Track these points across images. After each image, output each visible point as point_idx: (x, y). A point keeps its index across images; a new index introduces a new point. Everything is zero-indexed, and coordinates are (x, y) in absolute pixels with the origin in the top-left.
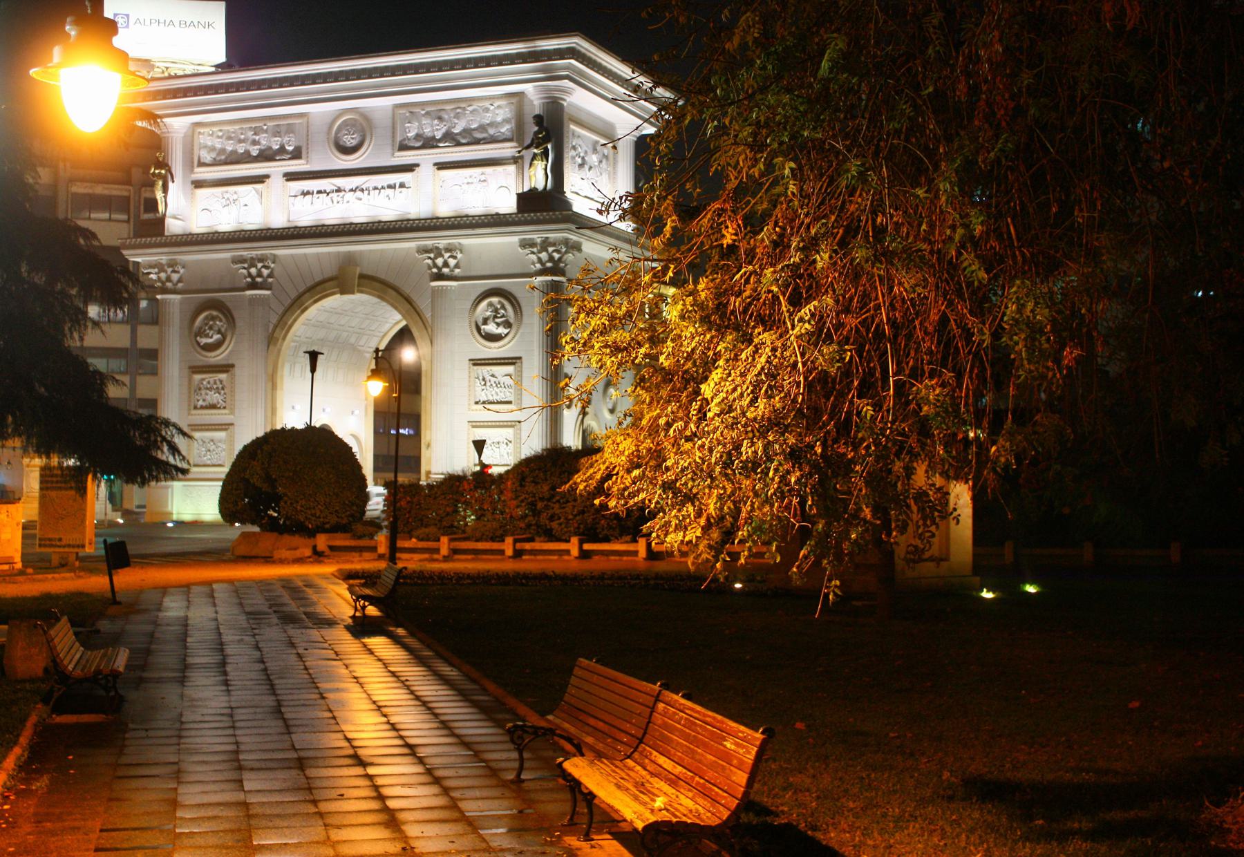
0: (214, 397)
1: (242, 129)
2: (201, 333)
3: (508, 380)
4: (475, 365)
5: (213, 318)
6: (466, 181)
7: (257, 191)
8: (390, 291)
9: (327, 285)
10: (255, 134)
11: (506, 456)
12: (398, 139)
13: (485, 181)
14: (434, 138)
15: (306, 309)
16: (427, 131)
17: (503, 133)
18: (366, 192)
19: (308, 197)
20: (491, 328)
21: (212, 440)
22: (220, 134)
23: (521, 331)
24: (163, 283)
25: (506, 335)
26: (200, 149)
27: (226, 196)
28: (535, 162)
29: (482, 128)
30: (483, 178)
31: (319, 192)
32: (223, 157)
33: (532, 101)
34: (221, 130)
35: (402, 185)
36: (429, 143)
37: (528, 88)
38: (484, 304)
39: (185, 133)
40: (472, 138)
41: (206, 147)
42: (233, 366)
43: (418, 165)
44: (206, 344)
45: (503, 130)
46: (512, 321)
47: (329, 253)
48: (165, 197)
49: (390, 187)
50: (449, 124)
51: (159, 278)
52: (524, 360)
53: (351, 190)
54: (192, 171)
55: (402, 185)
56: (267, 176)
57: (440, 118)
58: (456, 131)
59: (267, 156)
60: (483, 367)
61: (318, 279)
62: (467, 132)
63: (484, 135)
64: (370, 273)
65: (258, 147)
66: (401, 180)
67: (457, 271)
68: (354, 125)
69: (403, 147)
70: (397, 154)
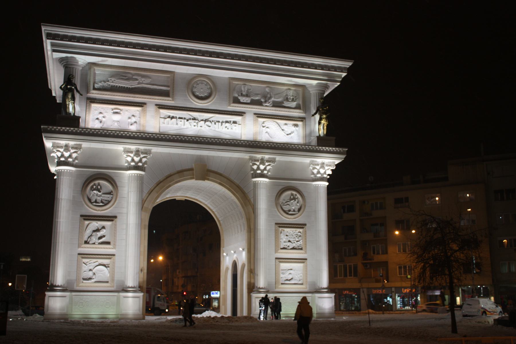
9: (185, 173)
15: (170, 186)
18: (213, 123)
24: (67, 158)
31: (180, 118)
33: (309, 91)
35: (235, 122)
37: (315, 82)
39: (83, 68)
42: (115, 217)
43: (244, 113)
49: (227, 122)
53: (202, 120)
54: (88, 92)
55: (235, 122)
56: (145, 104)
61: (179, 169)
64: (216, 170)
69: (236, 101)
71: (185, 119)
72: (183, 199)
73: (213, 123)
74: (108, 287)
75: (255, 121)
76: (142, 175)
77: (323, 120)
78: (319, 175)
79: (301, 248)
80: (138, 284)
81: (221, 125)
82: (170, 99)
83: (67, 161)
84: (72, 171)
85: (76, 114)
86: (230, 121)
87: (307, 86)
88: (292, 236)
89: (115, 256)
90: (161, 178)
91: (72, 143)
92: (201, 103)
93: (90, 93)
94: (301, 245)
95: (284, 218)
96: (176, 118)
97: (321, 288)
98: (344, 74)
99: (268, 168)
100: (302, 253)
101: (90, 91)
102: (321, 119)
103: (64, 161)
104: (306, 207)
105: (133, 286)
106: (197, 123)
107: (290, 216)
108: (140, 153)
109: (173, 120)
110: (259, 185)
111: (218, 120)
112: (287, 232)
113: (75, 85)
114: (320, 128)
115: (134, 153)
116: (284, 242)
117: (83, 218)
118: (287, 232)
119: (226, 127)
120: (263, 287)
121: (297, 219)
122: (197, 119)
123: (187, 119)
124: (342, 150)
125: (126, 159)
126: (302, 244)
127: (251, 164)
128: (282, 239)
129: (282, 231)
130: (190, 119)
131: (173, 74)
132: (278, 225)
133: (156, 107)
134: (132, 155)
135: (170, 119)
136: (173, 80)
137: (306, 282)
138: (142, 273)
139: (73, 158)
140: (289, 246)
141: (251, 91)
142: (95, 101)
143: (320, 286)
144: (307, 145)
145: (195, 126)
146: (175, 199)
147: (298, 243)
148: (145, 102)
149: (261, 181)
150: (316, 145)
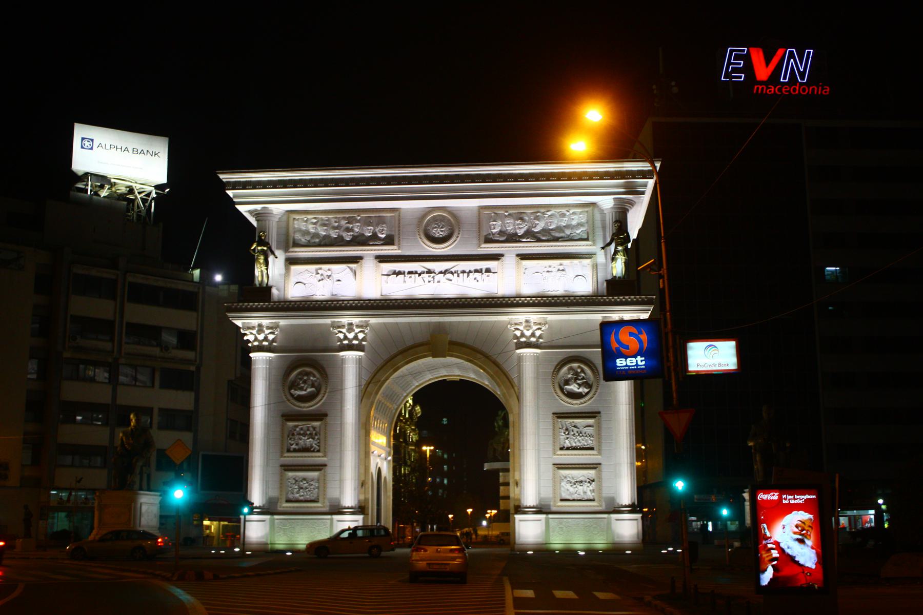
0: (309, 441)
1: (336, 218)
2: (294, 385)
3: (589, 430)
4: (558, 417)
5: (308, 374)
6: (546, 270)
7: (351, 269)
8: (479, 356)
10: (348, 223)
11: (589, 493)
12: (485, 234)
13: (563, 270)
14: (516, 234)
16: (510, 229)
17: (579, 234)
18: (456, 275)
19: (401, 277)
20: (574, 387)
21: (305, 479)
22: (316, 220)
23: (599, 391)
24: (261, 342)
25: (587, 393)
26: (295, 232)
27: (320, 272)
28: (617, 256)
29: (559, 229)
30: (561, 268)
32: (317, 240)
34: (315, 218)
35: (488, 270)
36: (513, 238)
38: (565, 369)
39: (280, 218)
40: (549, 236)
41: (300, 230)
42: (326, 415)
43: (502, 255)
44: (299, 396)
45: (577, 232)
46: (590, 383)
47: (405, 323)
48: (267, 269)
49: (476, 271)
50: (531, 225)
51: (256, 339)
52: (602, 412)
53: (441, 273)
55: (488, 270)
57: (522, 219)
58: (535, 230)
59: (360, 241)
60: (566, 420)
62: (545, 231)
63: (562, 235)
65: (351, 233)
66: (487, 267)
67: (541, 340)
68: (443, 221)
69: (488, 240)
70: (483, 245)
71: (416, 273)
72: (458, 378)
73: (455, 274)
74: (318, 507)
75: (518, 264)
76: (359, 356)
77: (619, 254)
80: (356, 502)
81: (468, 277)
82: (395, 247)
83: (260, 345)
84: (272, 357)
85: (270, 283)
86: (481, 269)
87: (598, 204)
89: (326, 467)
90: (386, 356)
91: (266, 322)
92: (439, 248)
93: (289, 252)
95: (564, 403)
96: (404, 273)
97: (622, 505)
98: (651, 183)
99: (538, 333)
100: (593, 455)
101: (288, 249)
102: (616, 252)
103: (258, 346)
104: (600, 388)
105: (350, 506)
106: (433, 277)
108: (354, 328)
109: (399, 276)
110: (524, 358)
111: (463, 269)
113: (266, 244)
114: (614, 266)
115: (346, 327)
117: (284, 418)
119: (475, 279)
120: (532, 505)
122: (432, 271)
123: (419, 272)
124: (646, 298)
125: (337, 335)
127: (514, 330)
130: (424, 273)
131: (398, 212)
132: (556, 415)
133: (376, 261)
134: (344, 330)
135: (395, 275)
136: (399, 220)
137: (600, 497)
138: (363, 488)
139: (269, 340)
142: (299, 261)
143: (620, 504)
144: (599, 296)
145: (429, 282)
146: (446, 379)
148: (361, 255)
149: (527, 353)
150: (605, 294)
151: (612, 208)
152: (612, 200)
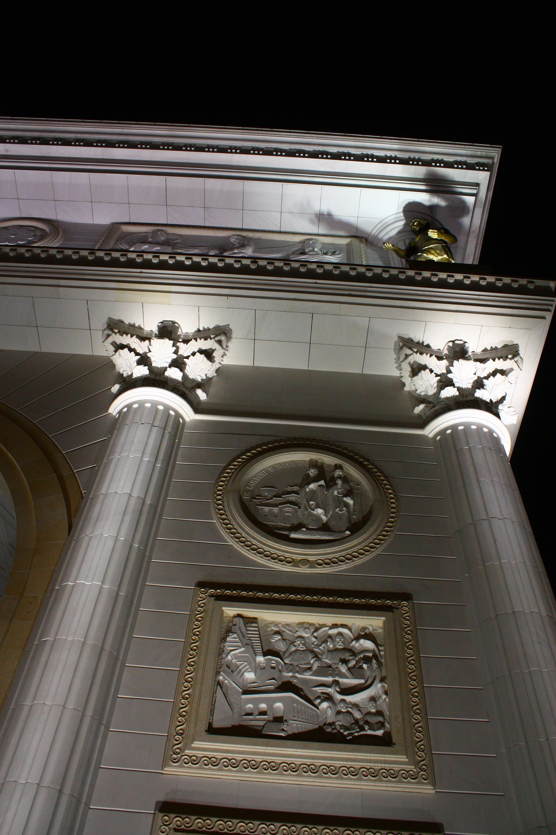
78: (449, 392)
79: (380, 733)
88: (310, 656)
94: (379, 713)
107: (297, 553)
112: (277, 633)
116: (246, 692)
118: (277, 633)
121: (343, 567)
126: (386, 713)
128: (231, 669)
129: (240, 622)
132: (212, 591)
140: (279, 720)
141: (178, 241)
147: (355, 706)
151: (399, 232)
152: (402, 214)
